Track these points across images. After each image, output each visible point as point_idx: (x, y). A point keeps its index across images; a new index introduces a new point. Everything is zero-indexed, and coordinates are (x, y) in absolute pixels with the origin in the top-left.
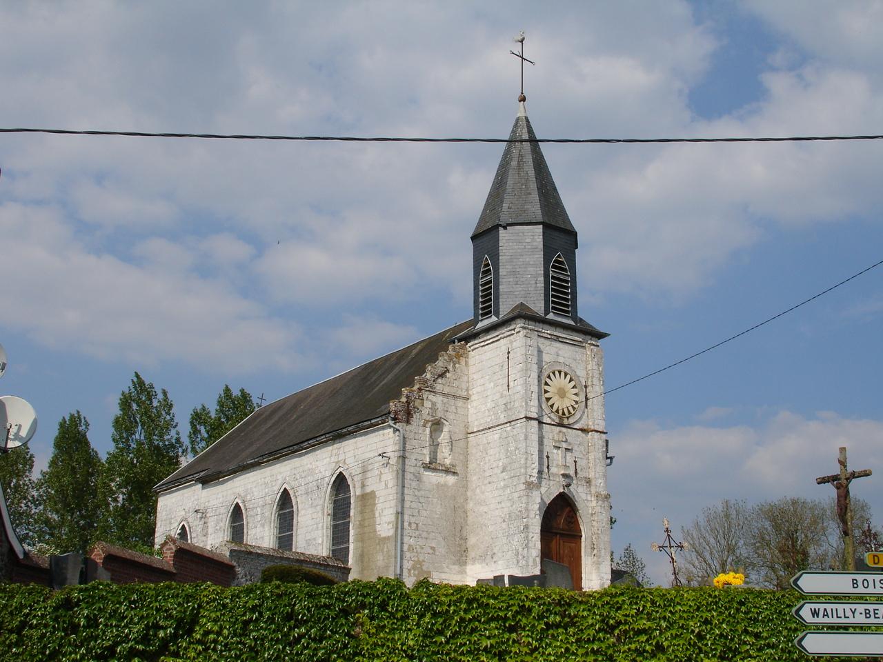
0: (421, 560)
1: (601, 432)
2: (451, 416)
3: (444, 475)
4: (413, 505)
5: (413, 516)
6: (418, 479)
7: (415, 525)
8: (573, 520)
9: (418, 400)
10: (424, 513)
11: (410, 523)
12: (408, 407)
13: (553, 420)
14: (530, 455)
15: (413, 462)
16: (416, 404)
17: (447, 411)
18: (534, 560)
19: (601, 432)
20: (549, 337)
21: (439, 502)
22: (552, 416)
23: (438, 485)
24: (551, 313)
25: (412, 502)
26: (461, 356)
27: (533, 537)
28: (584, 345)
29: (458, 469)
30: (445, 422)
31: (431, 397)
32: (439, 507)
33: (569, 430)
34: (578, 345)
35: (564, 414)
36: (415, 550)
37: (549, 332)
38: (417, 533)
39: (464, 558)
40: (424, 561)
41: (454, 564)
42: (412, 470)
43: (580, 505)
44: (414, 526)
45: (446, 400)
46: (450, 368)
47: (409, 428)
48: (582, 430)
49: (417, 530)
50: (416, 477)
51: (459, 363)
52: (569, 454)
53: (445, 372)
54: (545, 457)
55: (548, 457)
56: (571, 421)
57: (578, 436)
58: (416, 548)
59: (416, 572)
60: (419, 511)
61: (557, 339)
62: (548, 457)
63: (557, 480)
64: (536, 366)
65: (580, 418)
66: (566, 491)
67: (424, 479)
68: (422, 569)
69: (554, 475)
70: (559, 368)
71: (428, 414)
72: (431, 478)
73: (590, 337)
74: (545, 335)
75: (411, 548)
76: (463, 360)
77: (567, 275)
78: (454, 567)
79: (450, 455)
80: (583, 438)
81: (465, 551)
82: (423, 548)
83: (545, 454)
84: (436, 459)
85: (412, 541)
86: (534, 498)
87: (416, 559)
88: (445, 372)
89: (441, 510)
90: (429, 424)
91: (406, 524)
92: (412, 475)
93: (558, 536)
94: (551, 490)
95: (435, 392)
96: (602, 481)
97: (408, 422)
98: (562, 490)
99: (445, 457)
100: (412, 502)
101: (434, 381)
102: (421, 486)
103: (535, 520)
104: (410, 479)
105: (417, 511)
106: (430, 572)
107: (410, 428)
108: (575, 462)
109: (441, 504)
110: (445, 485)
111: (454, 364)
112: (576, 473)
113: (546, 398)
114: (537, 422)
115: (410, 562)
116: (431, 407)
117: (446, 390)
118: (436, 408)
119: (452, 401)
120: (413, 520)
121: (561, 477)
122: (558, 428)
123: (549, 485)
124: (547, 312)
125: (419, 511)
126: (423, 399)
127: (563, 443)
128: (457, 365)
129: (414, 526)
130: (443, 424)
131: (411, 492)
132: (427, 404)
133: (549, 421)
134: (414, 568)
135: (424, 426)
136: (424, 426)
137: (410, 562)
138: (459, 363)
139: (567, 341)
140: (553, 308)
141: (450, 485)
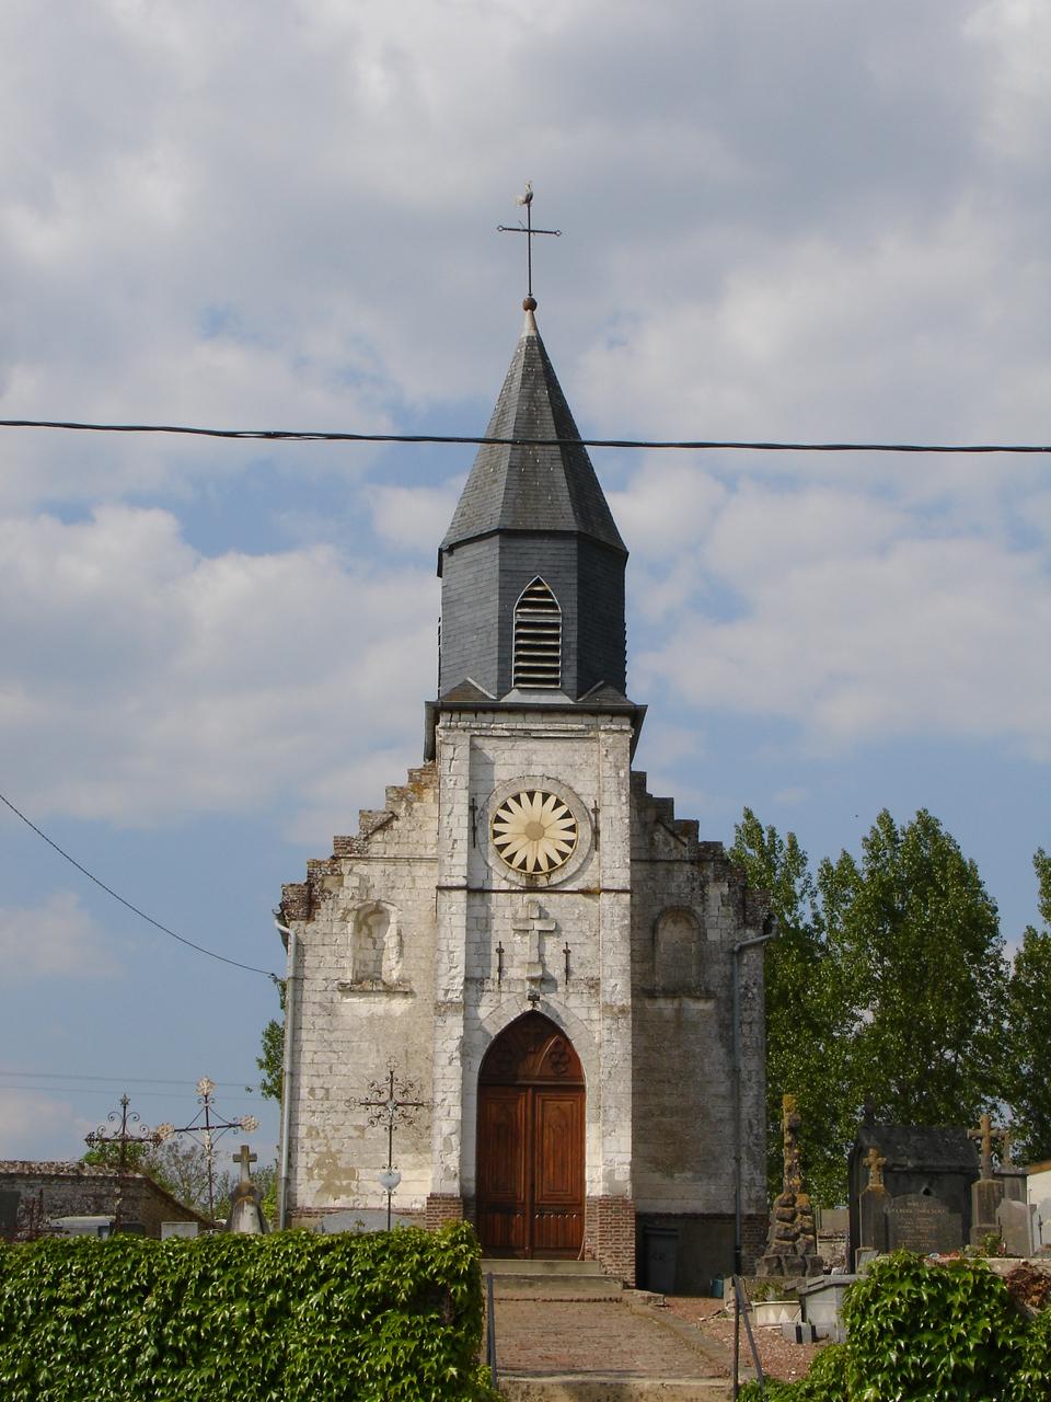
0: (333, 1150)
1: (617, 891)
2: (400, 895)
3: (386, 999)
4: (317, 1058)
5: (318, 1076)
6: (330, 1011)
7: (323, 1091)
8: (566, 1059)
9: (332, 878)
10: (344, 1069)
11: (312, 1091)
12: (310, 892)
13: (512, 882)
14: (445, 954)
15: (320, 984)
16: (327, 884)
17: (393, 888)
18: (447, 1141)
19: (617, 891)
20: (507, 733)
21: (374, 1047)
22: (512, 876)
23: (371, 1019)
24: (515, 692)
25: (315, 1053)
26: (426, 786)
27: (444, 1100)
28: (592, 734)
29: (415, 986)
30: (389, 907)
31: (361, 868)
32: (374, 1055)
33: (554, 897)
34: (580, 736)
35: (537, 867)
36: (322, 1135)
37: (504, 726)
38: (327, 1104)
39: (426, 1141)
40: (340, 1152)
41: (404, 1152)
42: (318, 998)
43: (572, 1033)
44: (320, 1093)
45: (390, 868)
46: (401, 811)
47: (311, 927)
48: (586, 892)
49: (327, 1099)
50: (324, 1008)
51: (420, 799)
52: (550, 942)
53: (389, 821)
54: (493, 952)
55: (500, 951)
56: (555, 879)
57: (575, 904)
58: (323, 1131)
59: (325, 1172)
60: (331, 1068)
61: (527, 734)
62: (500, 951)
63: (519, 990)
64: (466, 794)
65: (580, 870)
66: (539, 1008)
67: (343, 1010)
68: (336, 1166)
69: (510, 982)
70: (529, 788)
71: (352, 898)
72: (359, 1007)
73: (609, 718)
74: (499, 733)
75: (313, 1132)
76: (429, 795)
77: (557, 614)
78: (404, 1156)
79: (397, 962)
80: (585, 906)
81: (428, 1128)
82: (339, 1130)
83: (495, 946)
84: (381, 973)
85: (316, 1121)
86: (447, 1031)
87: (325, 1149)
88: (389, 821)
89: (377, 1061)
90: (351, 918)
91: (304, 1092)
92: (317, 1007)
93: (530, 1091)
94: (499, 1010)
95: (368, 859)
96: (619, 982)
97: (309, 917)
98: (528, 1007)
99: (392, 969)
100: (315, 1053)
101: (366, 839)
102: (335, 1024)
103: (450, 1069)
104: (313, 1015)
105: (327, 1066)
106: (353, 1170)
107: (314, 927)
108: (567, 952)
109: (378, 1051)
110: (388, 1016)
111: (409, 803)
112: (568, 971)
113: (498, 846)
114: (465, 892)
115: (312, 1155)
116: (357, 885)
117: (392, 851)
118: (369, 885)
119: (404, 869)
120: (318, 1083)
121: (528, 983)
122: (527, 896)
123: (499, 1001)
124: (503, 690)
125: (331, 1068)
126: (341, 875)
127: (535, 922)
128: (416, 805)
129: (320, 1093)
130: (388, 911)
131: (315, 1036)
132: (351, 882)
133: (505, 886)
134: (319, 1164)
135: (343, 919)
136: (343, 919)
137: (312, 1155)
138: (420, 799)
139: (551, 735)
140: (518, 680)
141: (398, 1015)
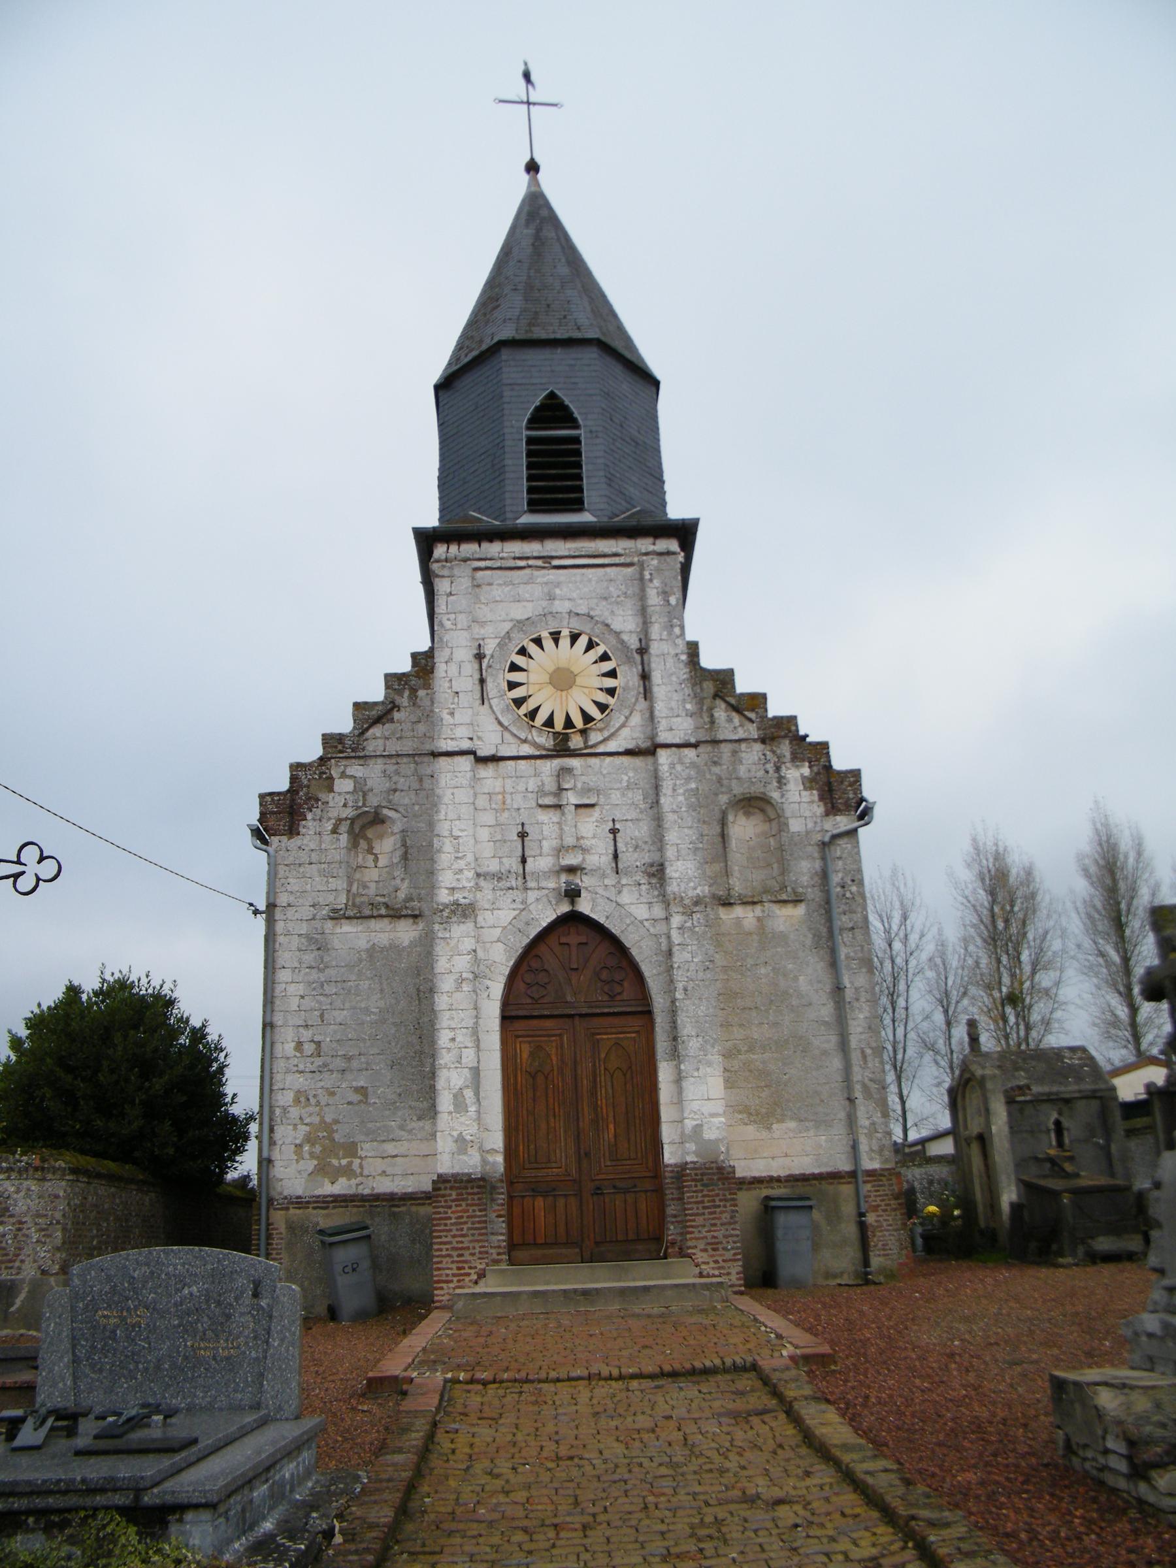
0: (328, 1119)
7: (313, 1046)
17: (395, 790)
23: (372, 951)
25: (302, 997)
30: (391, 814)
31: (356, 770)
35: (569, 723)
38: (319, 1062)
40: (336, 1122)
41: (419, 1119)
46: (404, 701)
53: (392, 709)
59: (318, 1149)
60: (322, 1016)
67: (336, 943)
69: (537, 876)
71: (345, 805)
78: (421, 1124)
87: (316, 1120)
89: (381, 1004)
90: (344, 828)
98: (565, 908)
103: (457, 995)
106: (354, 1144)
107: (299, 843)
108: (614, 832)
109: (382, 990)
110: (394, 947)
111: (414, 691)
117: (393, 747)
122: (557, 763)
123: (524, 902)
125: (322, 1016)
129: (309, 1048)
132: (343, 786)
134: (310, 1139)
136: (334, 831)
